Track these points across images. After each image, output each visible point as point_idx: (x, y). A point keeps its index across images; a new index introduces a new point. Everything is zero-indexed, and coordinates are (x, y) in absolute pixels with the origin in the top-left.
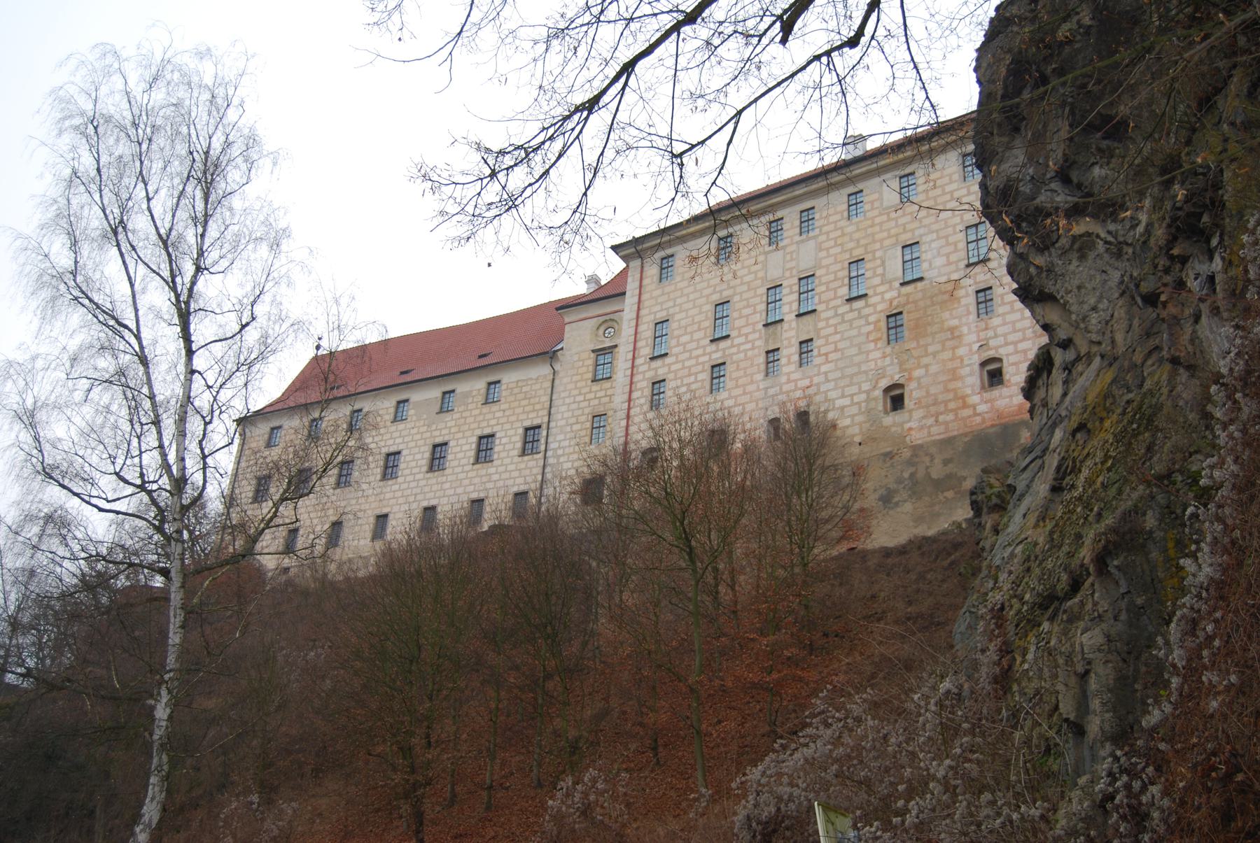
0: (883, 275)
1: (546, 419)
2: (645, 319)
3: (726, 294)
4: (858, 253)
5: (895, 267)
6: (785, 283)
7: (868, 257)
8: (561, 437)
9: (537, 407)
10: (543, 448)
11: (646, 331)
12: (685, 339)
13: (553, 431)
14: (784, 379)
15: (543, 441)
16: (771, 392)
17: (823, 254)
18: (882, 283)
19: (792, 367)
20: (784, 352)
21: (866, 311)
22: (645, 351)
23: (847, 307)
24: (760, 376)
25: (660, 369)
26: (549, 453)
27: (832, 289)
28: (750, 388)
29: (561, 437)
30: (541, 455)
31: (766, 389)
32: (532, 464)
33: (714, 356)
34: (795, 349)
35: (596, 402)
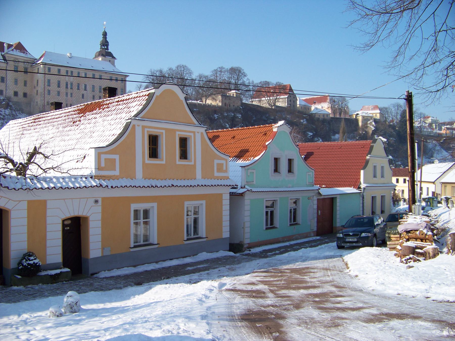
0: (82, 88)
1: (5, 76)
2: (46, 78)
3: (60, 80)
4: (79, 82)
5: (83, 87)
6: (69, 82)
7: (80, 84)
8: (9, 81)
9: (3, 73)
10: (5, 82)
11: (46, 81)
12: (53, 85)
13: (7, 79)
14: (68, 98)
15: (5, 81)
16: (67, 99)
17: (74, 80)
18: (82, 89)
19: (70, 97)
20: (68, 94)
21: (80, 92)
22: (46, 84)
23: (77, 90)
24: (65, 96)
25: (50, 88)
26: (7, 84)
27: (75, 87)
28: (64, 97)
29: (9, 81)
30: (5, 84)
31: (66, 98)
32: (3, 85)
33: (58, 90)
34: (70, 94)
35: (15, 76)
